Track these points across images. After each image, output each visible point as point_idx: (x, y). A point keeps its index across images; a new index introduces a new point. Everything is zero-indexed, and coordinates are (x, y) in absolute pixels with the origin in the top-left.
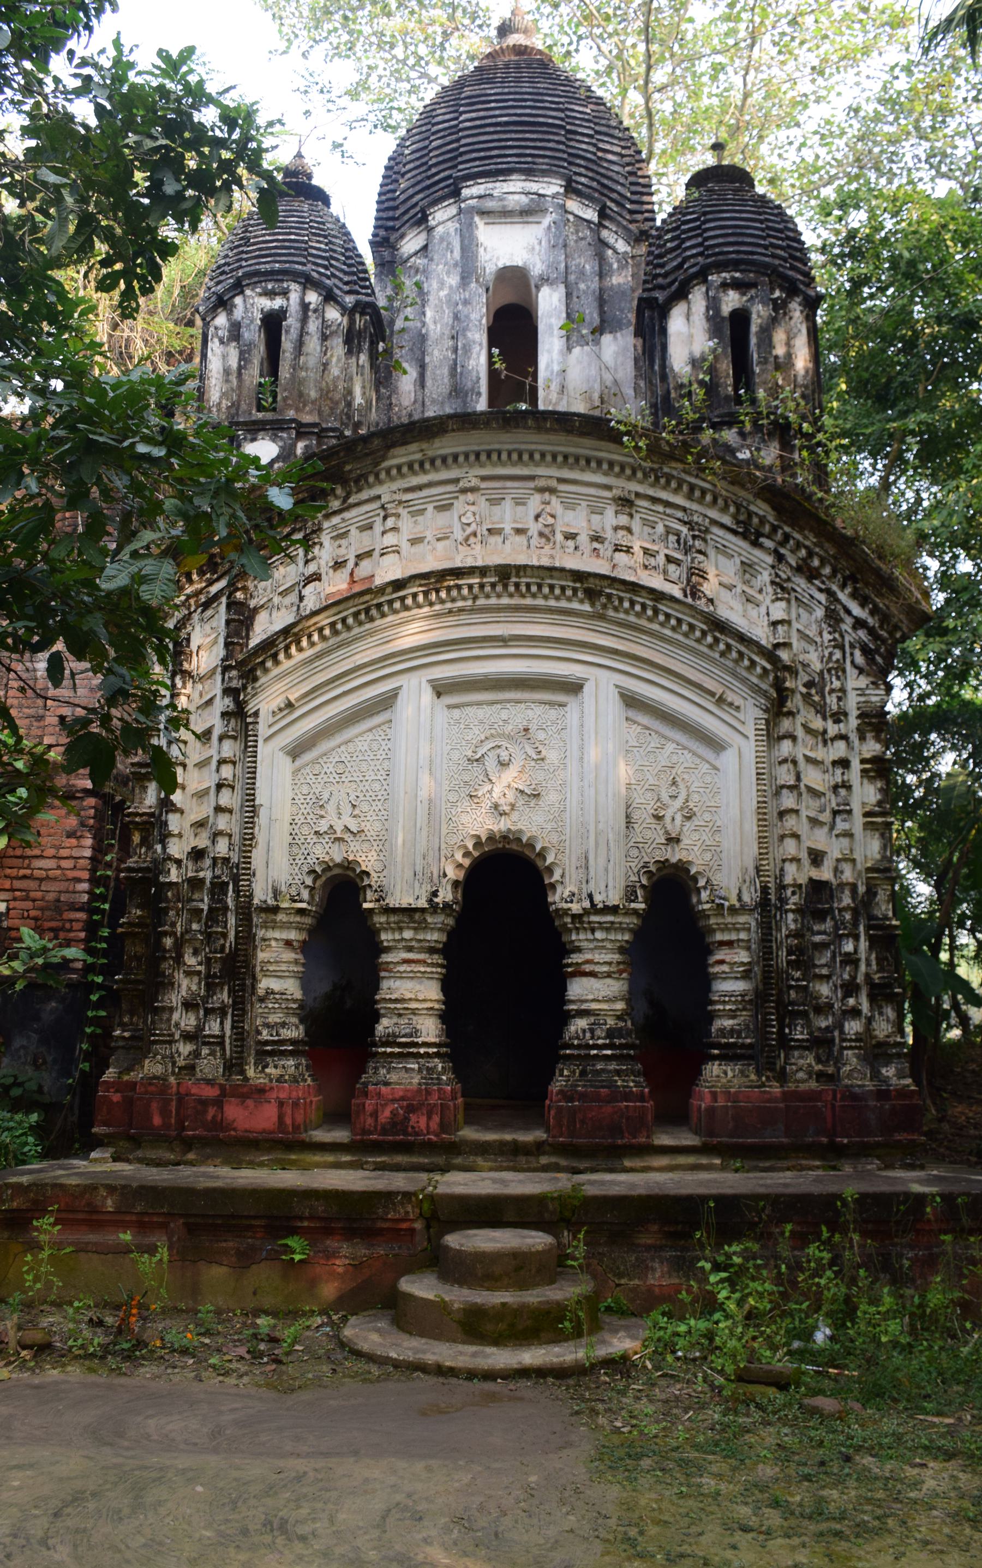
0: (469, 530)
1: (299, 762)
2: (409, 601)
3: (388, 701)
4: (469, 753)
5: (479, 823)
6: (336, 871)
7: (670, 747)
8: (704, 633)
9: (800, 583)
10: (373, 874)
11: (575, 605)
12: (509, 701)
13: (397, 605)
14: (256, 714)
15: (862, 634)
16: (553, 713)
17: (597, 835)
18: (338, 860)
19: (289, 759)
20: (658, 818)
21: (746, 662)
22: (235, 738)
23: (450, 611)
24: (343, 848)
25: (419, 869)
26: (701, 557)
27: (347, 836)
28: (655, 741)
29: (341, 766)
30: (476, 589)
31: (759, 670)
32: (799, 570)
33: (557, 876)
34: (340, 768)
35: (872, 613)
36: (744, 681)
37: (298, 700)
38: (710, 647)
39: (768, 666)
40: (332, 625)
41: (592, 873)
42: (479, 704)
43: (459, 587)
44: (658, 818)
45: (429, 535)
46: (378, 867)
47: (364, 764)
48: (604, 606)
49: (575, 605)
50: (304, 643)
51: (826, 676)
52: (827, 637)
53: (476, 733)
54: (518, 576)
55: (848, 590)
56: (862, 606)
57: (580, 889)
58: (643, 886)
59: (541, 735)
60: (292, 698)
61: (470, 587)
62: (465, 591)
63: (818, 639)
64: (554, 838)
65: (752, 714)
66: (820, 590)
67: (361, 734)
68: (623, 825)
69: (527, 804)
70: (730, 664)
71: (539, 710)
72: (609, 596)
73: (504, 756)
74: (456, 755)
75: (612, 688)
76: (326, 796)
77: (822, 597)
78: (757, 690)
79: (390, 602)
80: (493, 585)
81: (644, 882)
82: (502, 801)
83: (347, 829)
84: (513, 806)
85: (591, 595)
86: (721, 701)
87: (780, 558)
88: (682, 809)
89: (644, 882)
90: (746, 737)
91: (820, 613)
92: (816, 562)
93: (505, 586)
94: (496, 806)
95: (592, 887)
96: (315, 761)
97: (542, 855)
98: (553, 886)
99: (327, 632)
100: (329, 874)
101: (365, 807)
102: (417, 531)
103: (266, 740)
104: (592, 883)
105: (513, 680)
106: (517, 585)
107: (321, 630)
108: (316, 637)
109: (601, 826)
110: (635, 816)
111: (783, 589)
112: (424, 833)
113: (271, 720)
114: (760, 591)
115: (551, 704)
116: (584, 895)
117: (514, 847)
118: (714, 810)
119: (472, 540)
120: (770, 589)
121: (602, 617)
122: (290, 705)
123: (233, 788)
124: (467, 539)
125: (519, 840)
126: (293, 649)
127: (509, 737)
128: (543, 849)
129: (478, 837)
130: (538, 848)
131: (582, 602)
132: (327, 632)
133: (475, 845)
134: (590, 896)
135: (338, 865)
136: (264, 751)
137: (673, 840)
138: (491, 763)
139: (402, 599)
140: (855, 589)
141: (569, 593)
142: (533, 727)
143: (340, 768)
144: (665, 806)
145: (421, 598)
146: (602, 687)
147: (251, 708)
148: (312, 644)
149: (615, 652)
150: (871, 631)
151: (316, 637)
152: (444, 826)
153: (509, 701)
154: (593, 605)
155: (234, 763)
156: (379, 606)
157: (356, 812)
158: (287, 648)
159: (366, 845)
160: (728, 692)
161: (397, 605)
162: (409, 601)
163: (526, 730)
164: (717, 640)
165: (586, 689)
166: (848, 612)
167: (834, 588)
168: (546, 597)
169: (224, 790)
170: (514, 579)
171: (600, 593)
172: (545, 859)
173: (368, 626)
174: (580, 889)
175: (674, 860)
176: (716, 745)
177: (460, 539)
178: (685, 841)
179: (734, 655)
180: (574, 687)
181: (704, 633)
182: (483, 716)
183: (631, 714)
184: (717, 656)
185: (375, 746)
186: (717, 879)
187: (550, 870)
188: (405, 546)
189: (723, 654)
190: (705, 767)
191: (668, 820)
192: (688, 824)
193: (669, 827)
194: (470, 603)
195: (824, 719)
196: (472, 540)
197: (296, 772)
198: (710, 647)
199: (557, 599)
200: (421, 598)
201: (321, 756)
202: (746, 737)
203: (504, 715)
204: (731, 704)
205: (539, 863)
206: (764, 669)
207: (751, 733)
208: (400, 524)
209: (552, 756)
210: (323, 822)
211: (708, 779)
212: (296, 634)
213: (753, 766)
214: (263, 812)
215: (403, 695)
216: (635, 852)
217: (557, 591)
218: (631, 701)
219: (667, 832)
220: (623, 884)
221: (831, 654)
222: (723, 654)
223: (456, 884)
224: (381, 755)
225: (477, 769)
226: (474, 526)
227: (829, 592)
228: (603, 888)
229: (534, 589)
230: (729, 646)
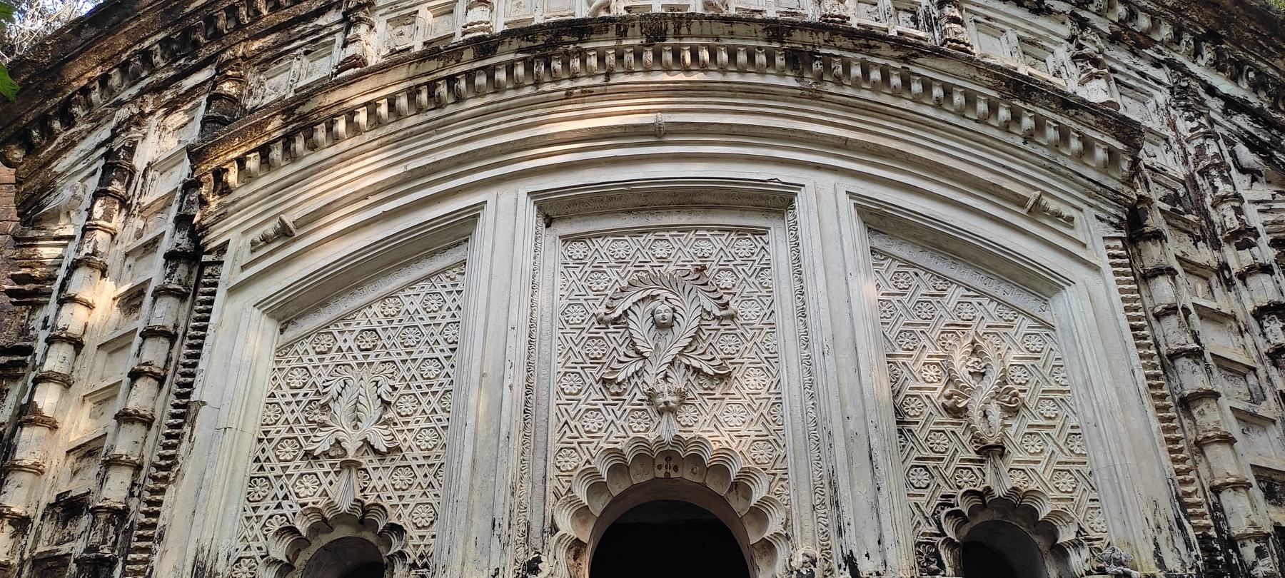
1: (290, 334)
2: (501, 76)
3: (460, 230)
4: (602, 310)
5: (622, 429)
6: (341, 532)
7: (955, 294)
8: (993, 108)
9: (1120, 56)
10: (411, 531)
11: (772, 80)
12: (668, 228)
13: (481, 80)
14: (222, 249)
15: (1242, 121)
16: (744, 246)
17: (849, 439)
18: (345, 507)
19: (271, 327)
20: (956, 412)
21: (1075, 144)
22: (182, 297)
23: (569, 94)
24: (356, 479)
25: (501, 513)
26: (956, 27)
27: (367, 461)
28: (925, 286)
29: (369, 338)
30: (611, 59)
31: (1100, 154)
32: (1114, 39)
33: (774, 525)
34: (369, 340)
35: (1255, 87)
36: (1073, 178)
37: (300, 224)
38: (1005, 128)
39: (1119, 146)
40: (371, 106)
41: (848, 515)
42: (617, 233)
43: (582, 55)
44: (956, 412)
46: (423, 516)
47: (411, 333)
48: (820, 79)
49: (772, 80)
50: (321, 134)
51: (1200, 180)
52: (1184, 126)
53: (614, 278)
54: (677, 35)
55: (1208, 55)
56: (1234, 79)
57: (826, 550)
58: (949, 543)
59: (726, 280)
60: (289, 219)
62: (593, 61)
63: (1170, 133)
64: (763, 453)
65: (1095, 234)
66: (1157, 64)
67: (410, 285)
68: (894, 427)
69: (708, 392)
70: (1045, 153)
71: (720, 241)
72: (827, 61)
73: (663, 309)
74: (576, 316)
75: (843, 198)
76: (334, 388)
77: (1162, 74)
78: (1097, 191)
79: (470, 76)
81: (951, 534)
82: (663, 387)
83: (368, 445)
84: (682, 395)
85: (797, 61)
86: (1036, 211)
87: (1083, 24)
88: (997, 395)
89: (951, 534)
90: (1096, 269)
91: (1162, 97)
92: (1144, 22)
93: (658, 56)
94: (651, 396)
95: (851, 542)
96: (324, 330)
97: (741, 487)
98: (768, 547)
99: (362, 117)
100: (325, 539)
101: (407, 406)
103: (234, 290)
104: (851, 535)
105: (674, 193)
107: (351, 113)
108: (341, 126)
109: (852, 425)
110: (912, 409)
111: (1096, 63)
112: (516, 443)
113: (247, 257)
114: (1057, 74)
115: (741, 231)
116: (837, 560)
117: (687, 474)
118: (1059, 396)
120: (1072, 68)
121: (815, 96)
122: (284, 233)
123: (161, 380)
125: (696, 459)
126: (299, 144)
127: (671, 284)
128: (746, 473)
129: (620, 453)
130: (734, 473)
131: (782, 74)
132: (362, 117)
133: (613, 470)
134: (850, 562)
135: (343, 518)
136: (224, 310)
137: (991, 451)
138: (640, 327)
139: (490, 71)
140: (1219, 53)
141: (761, 59)
142: (712, 268)
143: (369, 340)
144: (965, 392)
145: (520, 70)
146: (826, 203)
147: (214, 238)
148: (335, 138)
149: (843, 145)
150: (1256, 115)
151: (341, 126)
152: (554, 436)
153: (668, 228)
154: (800, 77)
155: (172, 338)
156: (451, 80)
157: (390, 414)
158: (288, 139)
159: (403, 475)
160: (1045, 199)
161: (481, 80)
162: (501, 76)
163: (701, 270)
164: (1016, 117)
165: (800, 202)
166: (1211, 91)
167: (1180, 58)
168: (723, 70)
169: (141, 383)
170: (670, 41)
171: (813, 56)
172: (748, 493)
173: (432, 115)
174: (826, 550)
175: (999, 492)
176: (1042, 285)
178: (1015, 456)
179: (1052, 134)
180: (778, 203)
181: (993, 108)
182: (624, 252)
183: (879, 243)
184: (1019, 141)
185: (433, 303)
186: (1095, 525)
187: (759, 514)
189: (1028, 137)
190: (1025, 325)
191: (976, 415)
192: (1015, 423)
193: (981, 428)
194: (600, 80)
195: (1216, 246)
197: (283, 350)
198: (1005, 128)
199: (742, 71)
200: (520, 70)
201: (335, 322)
202: (1096, 269)
203: (661, 250)
204: (1057, 215)
205: (738, 506)
206: (1111, 151)
207: (1104, 262)
209: (749, 311)
210: (323, 434)
211: (1035, 344)
212: (303, 117)
213: (1122, 316)
214: (203, 417)
215: (486, 218)
216: (920, 477)
217: (742, 58)
218: (877, 220)
219: (976, 438)
220: (911, 540)
221: (1201, 149)
222: (1028, 137)
223: (577, 547)
224: (444, 317)
225: (615, 338)
227: (1171, 64)
228: (872, 545)
229: (705, 55)
230: (1040, 125)
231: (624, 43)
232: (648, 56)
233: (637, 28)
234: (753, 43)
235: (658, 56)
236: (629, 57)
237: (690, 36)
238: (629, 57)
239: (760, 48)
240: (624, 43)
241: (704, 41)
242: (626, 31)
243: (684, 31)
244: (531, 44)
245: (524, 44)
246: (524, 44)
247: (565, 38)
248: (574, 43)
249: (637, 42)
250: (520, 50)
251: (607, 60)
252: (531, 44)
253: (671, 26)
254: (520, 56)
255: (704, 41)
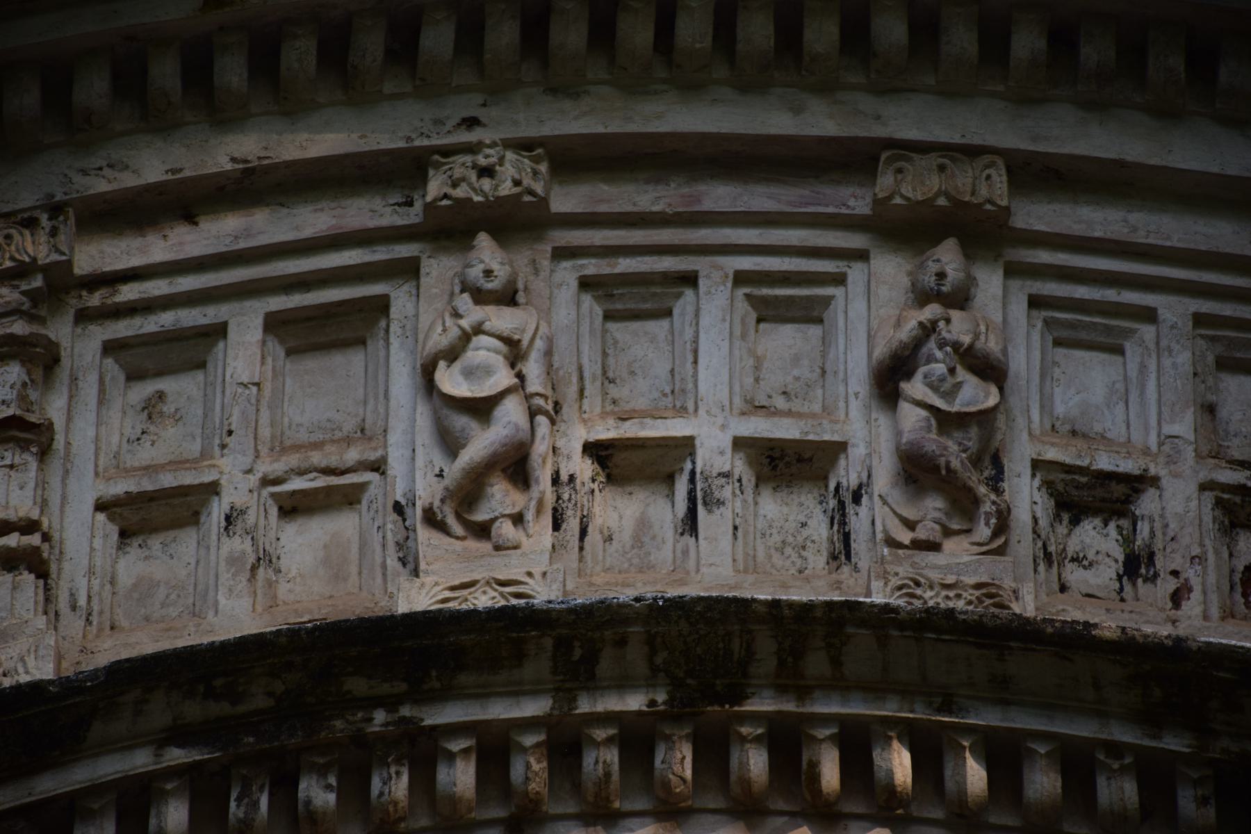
0: (481, 442)
43: (423, 751)
45: (237, 489)
54: (791, 681)
61: (494, 748)
80: (637, 740)
93: (714, 754)
102: (165, 454)
106: (787, 742)
119: (501, 497)
124: (468, 493)
177: (427, 491)
188: (81, 537)
196: (501, 497)
208: (55, 408)
226: (511, 413)
231: (585, 706)
232: (679, 761)
233: (636, 654)
234: (1082, 729)
235: (714, 754)
236: (602, 759)
237: (840, 685)
238: (602, 759)
239: (1114, 749)
240: (585, 706)
241: (889, 709)
242: (592, 658)
243: (816, 664)
244: (224, 708)
245: (193, 711)
246: (193, 711)
247: (357, 686)
248: (391, 704)
249: (634, 702)
250: (178, 735)
251: (517, 771)
252: (224, 708)
253: (766, 646)
254: (177, 756)
255: (889, 709)
